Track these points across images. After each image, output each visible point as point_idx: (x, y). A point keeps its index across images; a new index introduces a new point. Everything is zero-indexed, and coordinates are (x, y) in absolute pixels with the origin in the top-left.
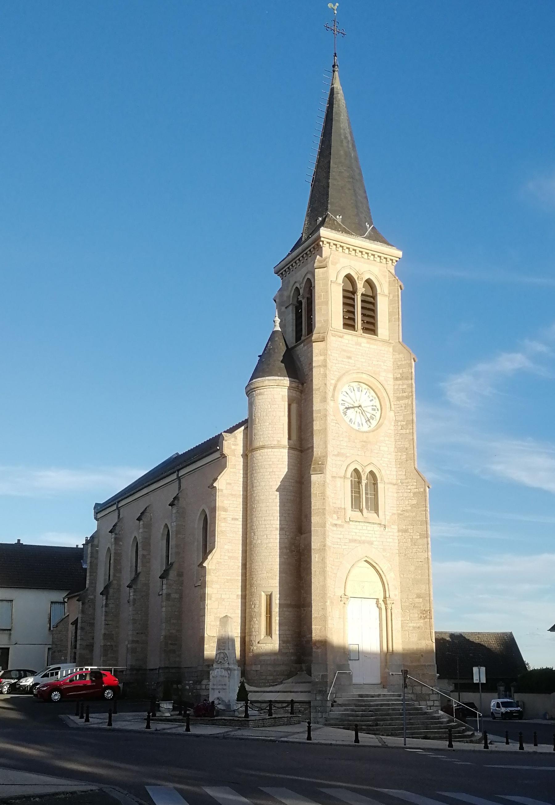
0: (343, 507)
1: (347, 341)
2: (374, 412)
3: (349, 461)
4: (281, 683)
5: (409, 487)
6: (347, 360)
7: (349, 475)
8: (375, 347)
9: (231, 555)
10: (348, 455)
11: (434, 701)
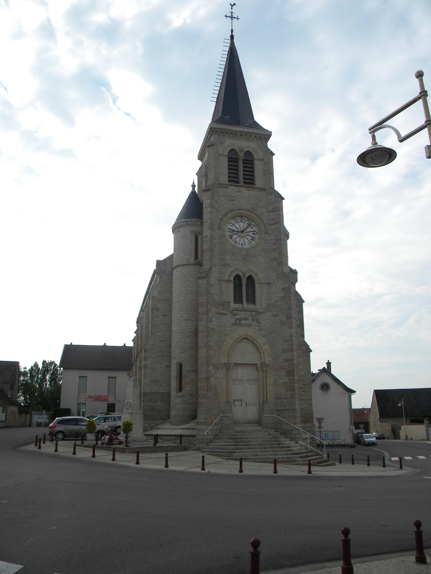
0: (227, 300)
1: (231, 190)
2: (254, 236)
3: (232, 269)
4: (189, 423)
5: (279, 285)
6: (231, 202)
7: (232, 279)
8: (253, 192)
9: (161, 339)
10: (232, 265)
11: (295, 434)
